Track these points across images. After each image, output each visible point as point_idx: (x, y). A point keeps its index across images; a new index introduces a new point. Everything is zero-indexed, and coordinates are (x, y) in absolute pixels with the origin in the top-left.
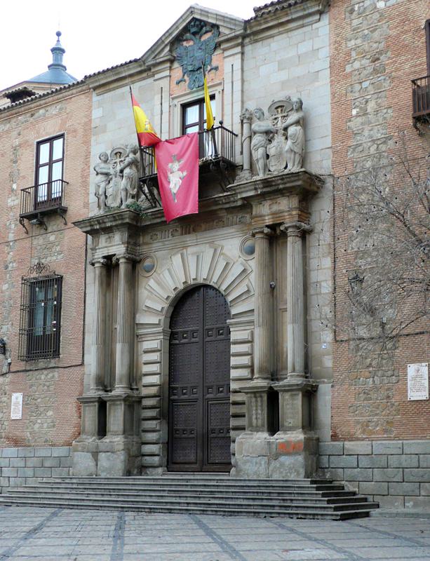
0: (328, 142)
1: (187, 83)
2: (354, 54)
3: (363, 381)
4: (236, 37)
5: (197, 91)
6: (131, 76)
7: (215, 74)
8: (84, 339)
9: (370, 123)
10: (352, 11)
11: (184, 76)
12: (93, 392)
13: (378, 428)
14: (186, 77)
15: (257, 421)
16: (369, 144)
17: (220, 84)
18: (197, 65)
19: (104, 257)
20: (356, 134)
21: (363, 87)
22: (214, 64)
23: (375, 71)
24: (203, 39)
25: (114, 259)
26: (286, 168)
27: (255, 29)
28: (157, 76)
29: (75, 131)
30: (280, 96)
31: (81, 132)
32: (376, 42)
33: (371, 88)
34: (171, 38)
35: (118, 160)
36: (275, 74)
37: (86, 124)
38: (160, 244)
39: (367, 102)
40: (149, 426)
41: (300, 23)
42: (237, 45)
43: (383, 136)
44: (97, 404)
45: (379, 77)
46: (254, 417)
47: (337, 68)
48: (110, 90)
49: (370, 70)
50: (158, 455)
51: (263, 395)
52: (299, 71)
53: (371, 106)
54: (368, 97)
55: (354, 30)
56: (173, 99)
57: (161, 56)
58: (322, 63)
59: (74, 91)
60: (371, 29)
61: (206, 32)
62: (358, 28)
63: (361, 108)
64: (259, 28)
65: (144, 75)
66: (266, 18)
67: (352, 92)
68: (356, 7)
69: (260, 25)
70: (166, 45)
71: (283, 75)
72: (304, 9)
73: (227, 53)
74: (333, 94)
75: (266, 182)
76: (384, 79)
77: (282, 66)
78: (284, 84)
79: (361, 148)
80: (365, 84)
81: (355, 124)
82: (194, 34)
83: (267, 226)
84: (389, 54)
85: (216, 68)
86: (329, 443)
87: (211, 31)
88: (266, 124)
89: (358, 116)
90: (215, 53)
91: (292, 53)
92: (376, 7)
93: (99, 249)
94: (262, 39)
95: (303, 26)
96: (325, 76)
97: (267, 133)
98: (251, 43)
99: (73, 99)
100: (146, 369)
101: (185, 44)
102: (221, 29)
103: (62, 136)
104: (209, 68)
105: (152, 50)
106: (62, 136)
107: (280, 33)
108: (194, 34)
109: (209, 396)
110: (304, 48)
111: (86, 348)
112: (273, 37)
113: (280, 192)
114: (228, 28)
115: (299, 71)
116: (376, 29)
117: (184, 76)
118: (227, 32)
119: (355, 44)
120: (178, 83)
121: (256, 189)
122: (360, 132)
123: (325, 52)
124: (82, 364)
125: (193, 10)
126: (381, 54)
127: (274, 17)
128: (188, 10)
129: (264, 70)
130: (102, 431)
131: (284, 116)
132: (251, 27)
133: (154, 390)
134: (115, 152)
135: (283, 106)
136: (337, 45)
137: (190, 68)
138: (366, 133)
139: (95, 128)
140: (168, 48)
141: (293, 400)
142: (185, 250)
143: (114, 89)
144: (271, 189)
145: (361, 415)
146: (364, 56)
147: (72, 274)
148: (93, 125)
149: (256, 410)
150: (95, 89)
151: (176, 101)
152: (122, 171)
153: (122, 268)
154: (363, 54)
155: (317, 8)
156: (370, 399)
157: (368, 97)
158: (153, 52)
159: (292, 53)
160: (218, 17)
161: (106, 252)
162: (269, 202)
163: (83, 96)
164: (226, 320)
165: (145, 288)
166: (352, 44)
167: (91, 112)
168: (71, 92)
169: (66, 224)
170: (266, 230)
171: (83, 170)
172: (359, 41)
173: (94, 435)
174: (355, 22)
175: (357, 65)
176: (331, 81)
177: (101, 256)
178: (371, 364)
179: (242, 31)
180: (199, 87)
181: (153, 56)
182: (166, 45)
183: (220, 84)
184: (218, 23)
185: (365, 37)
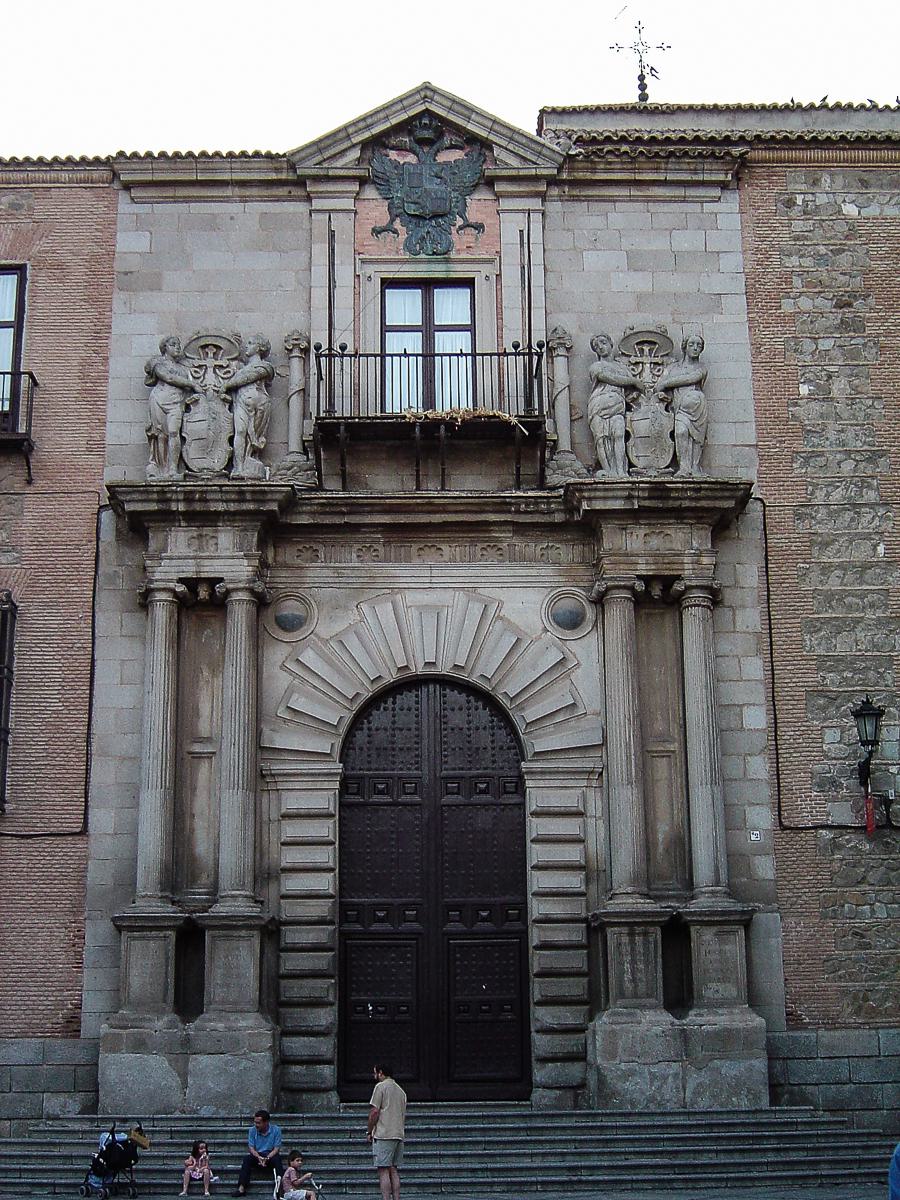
0: (750, 435)
1: (403, 237)
2: (797, 282)
3: (850, 910)
4: (536, 179)
5: (429, 262)
6: (243, 184)
7: (477, 239)
8: (88, 771)
9: (838, 417)
10: (790, 203)
11: (392, 221)
12: (150, 903)
13: (888, 1004)
14: (397, 224)
15: (636, 986)
16: (838, 456)
17: (490, 261)
18: (429, 207)
19: (181, 581)
20: (809, 431)
21: (820, 347)
22: (473, 216)
23: (844, 325)
24: (442, 157)
25: (219, 588)
26: (675, 462)
27: (580, 175)
28: (317, 204)
29: (60, 266)
30: (645, 321)
31: (79, 272)
32: (845, 274)
33: (836, 353)
34: (367, 135)
35: (210, 362)
36: (621, 275)
37: (95, 258)
38: (329, 573)
39: (830, 377)
40: (305, 993)
41: (680, 192)
42: (537, 195)
43: (866, 447)
44: (172, 934)
45: (853, 338)
46: (627, 977)
47: (761, 296)
48: (176, 200)
49: (835, 318)
50: (329, 1062)
51: (652, 929)
52: (676, 283)
53: (839, 387)
54: (832, 369)
55: (797, 239)
56: (363, 261)
57: (340, 163)
58: (729, 275)
59: (65, 176)
60: (831, 248)
61: (452, 147)
62: (806, 238)
63: (818, 386)
64: (589, 176)
65: (282, 191)
66: (610, 163)
67: (796, 351)
68: (799, 200)
69: (594, 170)
70: (354, 146)
71: (641, 283)
72: (695, 171)
73: (505, 204)
74: (757, 348)
75: (658, 490)
76: (865, 345)
77: (635, 262)
78: (641, 299)
79: (821, 461)
80: (826, 344)
81: (809, 412)
82: (421, 142)
83: (639, 577)
84: (871, 301)
85: (479, 227)
86: (785, 1034)
87: (461, 148)
88: (620, 371)
89: (811, 398)
90: (476, 196)
91: (659, 244)
92: (840, 212)
93: (171, 558)
94: (588, 199)
95: (684, 200)
96: (736, 309)
97: (630, 388)
98: (561, 198)
99: (54, 192)
100: (292, 857)
101: (393, 155)
102: (496, 151)
103: (19, 270)
104: (460, 222)
105: (319, 145)
106: (19, 270)
107: (631, 199)
108: (421, 142)
109: (450, 927)
110: (686, 241)
111: (93, 792)
112: (615, 201)
113: (679, 515)
114: (517, 155)
115: (676, 283)
116: (844, 251)
117: (392, 221)
118: (514, 162)
119: (800, 266)
120: (376, 232)
121: (629, 498)
122: (818, 429)
123: (734, 262)
124: (84, 832)
125: (429, 93)
126: (856, 299)
127: (630, 166)
128: (418, 91)
129: (591, 259)
130: (188, 998)
131: (655, 364)
132: (572, 170)
133: (320, 909)
134: (203, 342)
135: (655, 343)
136: (761, 255)
137: (412, 210)
138: (832, 435)
139: (126, 274)
140: (356, 154)
141: (723, 942)
142: (399, 596)
143: (187, 200)
144: (659, 505)
145: (851, 977)
146: (820, 292)
147: (47, 605)
148: (118, 266)
149: (633, 962)
150: (127, 187)
151: (370, 269)
152: (233, 390)
153: (240, 614)
154: (818, 287)
155: (721, 177)
156: (868, 946)
157: (832, 369)
158: (320, 151)
159: (659, 244)
160: (496, 127)
161: (189, 570)
162: (642, 532)
163: (88, 194)
164: (518, 762)
165: (283, 667)
166: (795, 260)
167: (114, 235)
168: (53, 175)
169: (29, 482)
170: (640, 586)
171: (86, 363)
172: (807, 262)
173: (161, 1013)
174: (799, 226)
175: (805, 303)
176: (750, 320)
177: (175, 577)
178: (864, 878)
179: (555, 172)
180: (434, 253)
181: (319, 158)
182: (354, 146)
183: (490, 261)
184: (492, 137)
185: (819, 258)
